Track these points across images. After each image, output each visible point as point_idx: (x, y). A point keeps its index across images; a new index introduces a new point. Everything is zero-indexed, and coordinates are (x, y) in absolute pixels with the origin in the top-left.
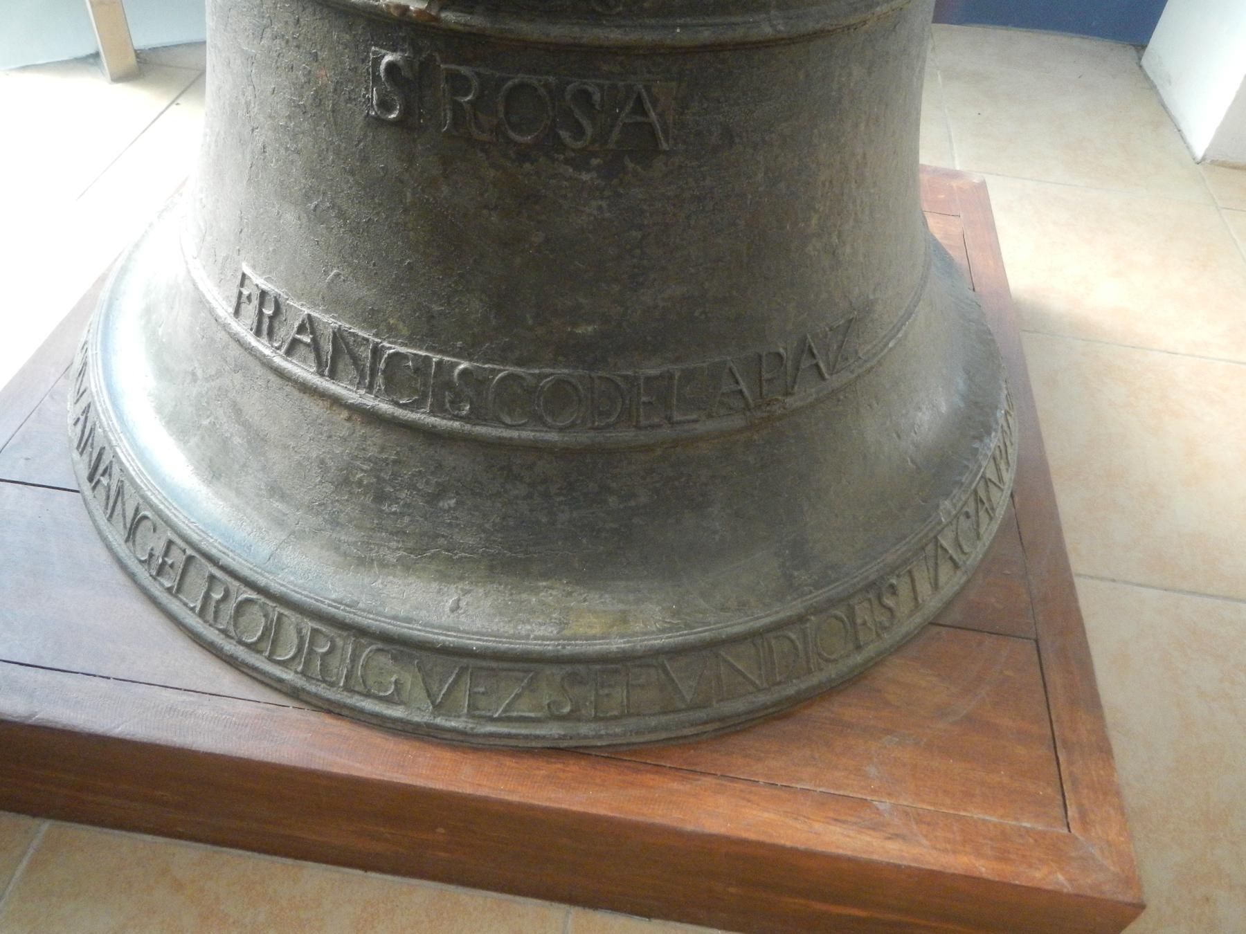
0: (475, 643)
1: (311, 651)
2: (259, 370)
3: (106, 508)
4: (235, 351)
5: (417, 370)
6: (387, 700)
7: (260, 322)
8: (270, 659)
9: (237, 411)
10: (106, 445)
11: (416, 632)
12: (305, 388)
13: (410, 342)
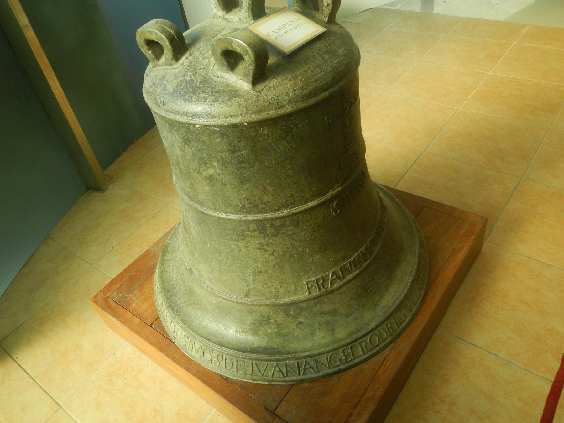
0: (405, 292)
1: (388, 329)
2: (324, 298)
3: (314, 370)
4: (312, 303)
5: (358, 258)
6: (404, 321)
7: (319, 287)
8: (383, 342)
9: (324, 313)
10: (298, 361)
11: (398, 302)
12: (340, 287)
13: (354, 254)
